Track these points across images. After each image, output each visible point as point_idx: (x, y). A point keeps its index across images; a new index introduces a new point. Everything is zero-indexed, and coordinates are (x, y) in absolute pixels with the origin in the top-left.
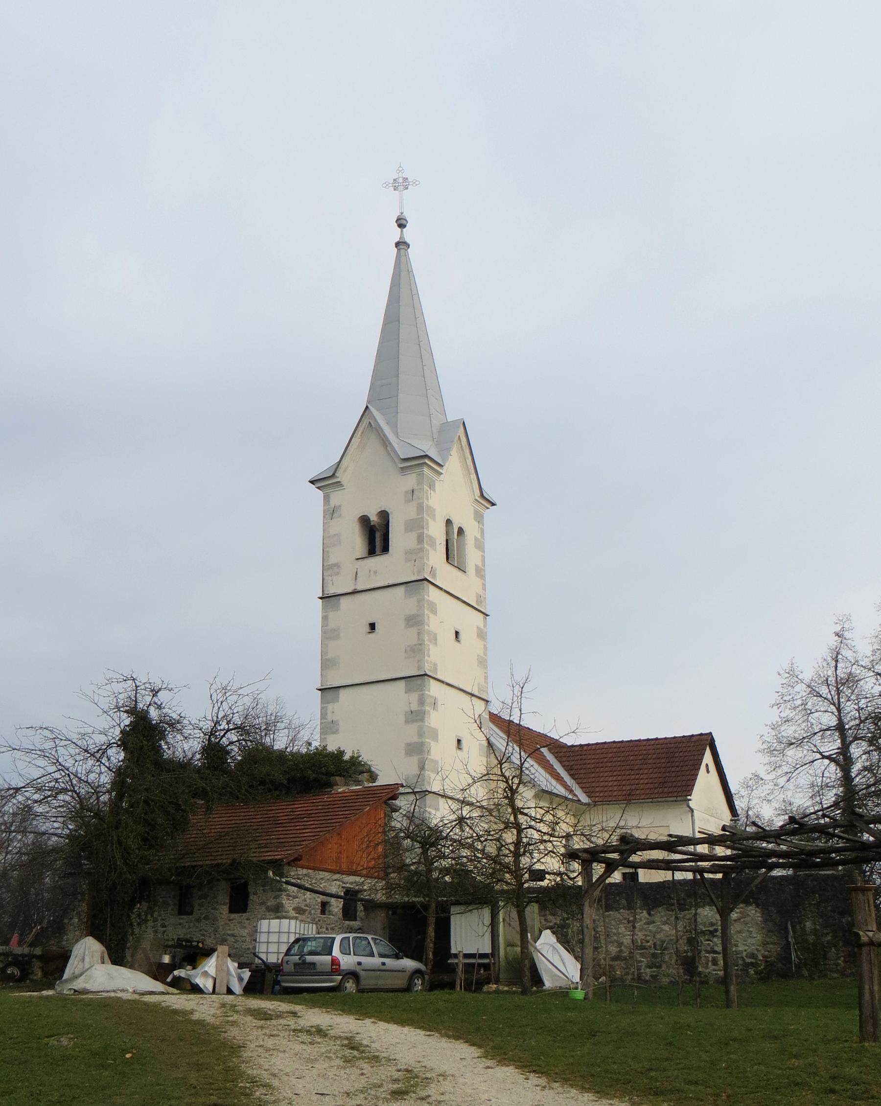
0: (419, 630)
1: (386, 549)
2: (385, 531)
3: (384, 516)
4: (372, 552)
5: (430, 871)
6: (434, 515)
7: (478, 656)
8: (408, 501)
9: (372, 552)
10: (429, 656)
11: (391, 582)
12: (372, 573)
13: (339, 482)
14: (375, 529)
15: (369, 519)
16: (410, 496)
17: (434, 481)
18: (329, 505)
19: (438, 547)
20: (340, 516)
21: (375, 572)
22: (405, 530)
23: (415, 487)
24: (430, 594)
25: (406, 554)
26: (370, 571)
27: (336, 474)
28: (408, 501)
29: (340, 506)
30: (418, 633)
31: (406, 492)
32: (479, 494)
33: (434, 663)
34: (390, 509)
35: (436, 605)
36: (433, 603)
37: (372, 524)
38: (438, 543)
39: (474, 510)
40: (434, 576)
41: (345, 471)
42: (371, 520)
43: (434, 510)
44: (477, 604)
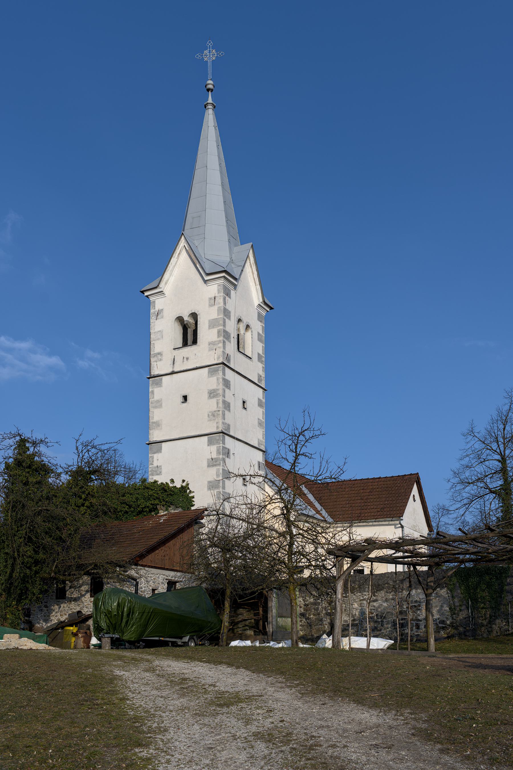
0: (217, 400)
1: (195, 342)
2: (194, 328)
3: (194, 316)
4: (185, 344)
5: (227, 568)
6: (230, 316)
7: (258, 419)
8: (211, 306)
9: (185, 344)
10: (263, 412)
11: (198, 365)
12: (185, 359)
13: (162, 291)
14: (187, 327)
15: (184, 319)
16: (213, 301)
17: (230, 291)
18: (155, 309)
19: (232, 339)
20: (162, 317)
21: (187, 359)
22: (209, 326)
23: (216, 295)
24: (226, 374)
25: (209, 344)
26: (184, 357)
27: (160, 286)
28: (211, 306)
29: (162, 310)
30: (217, 402)
31: (210, 299)
32: (262, 301)
33: (228, 424)
34: (198, 311)
35: (230, 382)
36: (228, 380)
37: (185, 323)
38: (232, 336)
39: (258, 312)
40: (229, 361)
41: (166, 283)
42: (185, 320)
43: (230, 312)
44: (259, 382)
